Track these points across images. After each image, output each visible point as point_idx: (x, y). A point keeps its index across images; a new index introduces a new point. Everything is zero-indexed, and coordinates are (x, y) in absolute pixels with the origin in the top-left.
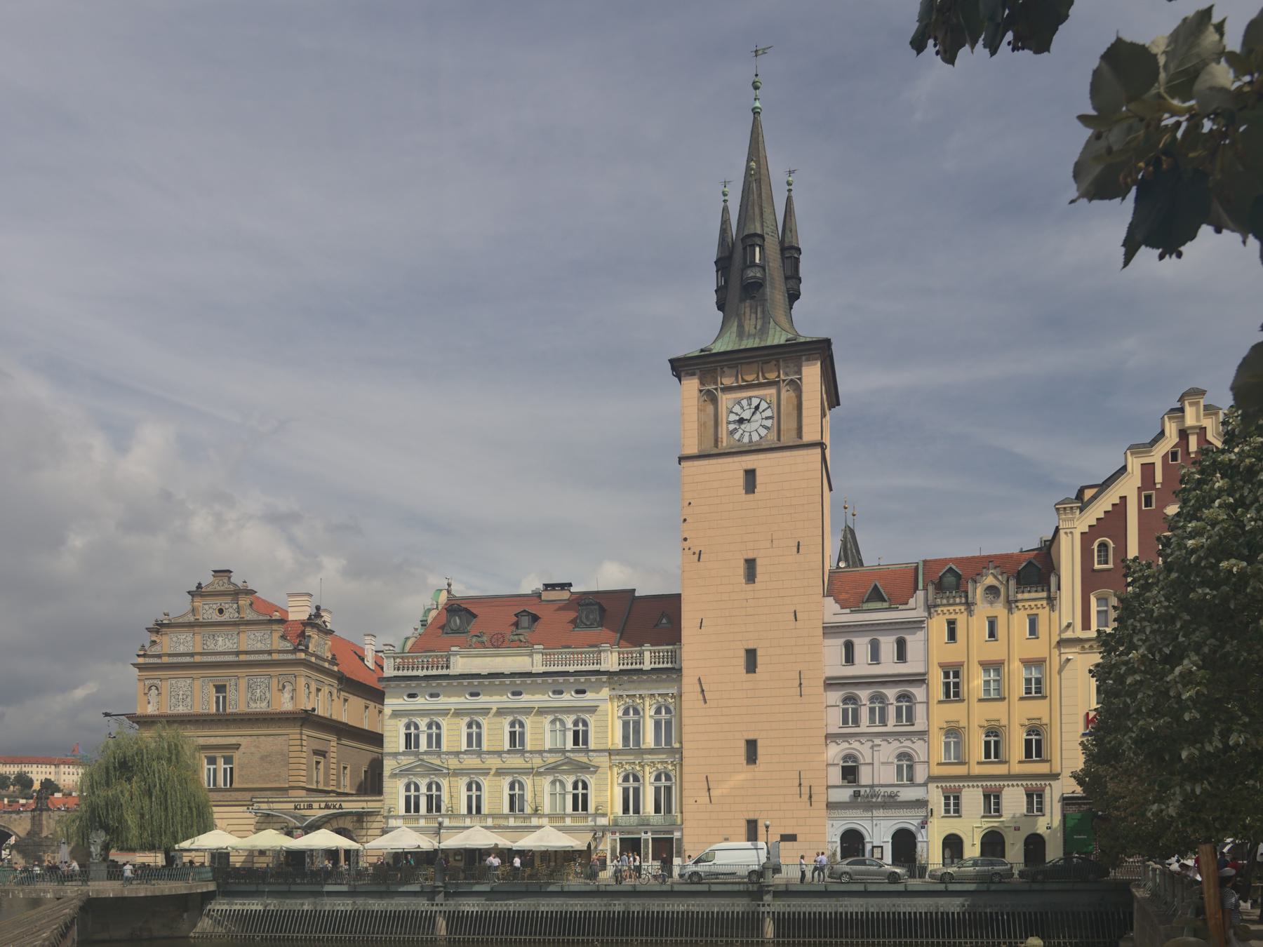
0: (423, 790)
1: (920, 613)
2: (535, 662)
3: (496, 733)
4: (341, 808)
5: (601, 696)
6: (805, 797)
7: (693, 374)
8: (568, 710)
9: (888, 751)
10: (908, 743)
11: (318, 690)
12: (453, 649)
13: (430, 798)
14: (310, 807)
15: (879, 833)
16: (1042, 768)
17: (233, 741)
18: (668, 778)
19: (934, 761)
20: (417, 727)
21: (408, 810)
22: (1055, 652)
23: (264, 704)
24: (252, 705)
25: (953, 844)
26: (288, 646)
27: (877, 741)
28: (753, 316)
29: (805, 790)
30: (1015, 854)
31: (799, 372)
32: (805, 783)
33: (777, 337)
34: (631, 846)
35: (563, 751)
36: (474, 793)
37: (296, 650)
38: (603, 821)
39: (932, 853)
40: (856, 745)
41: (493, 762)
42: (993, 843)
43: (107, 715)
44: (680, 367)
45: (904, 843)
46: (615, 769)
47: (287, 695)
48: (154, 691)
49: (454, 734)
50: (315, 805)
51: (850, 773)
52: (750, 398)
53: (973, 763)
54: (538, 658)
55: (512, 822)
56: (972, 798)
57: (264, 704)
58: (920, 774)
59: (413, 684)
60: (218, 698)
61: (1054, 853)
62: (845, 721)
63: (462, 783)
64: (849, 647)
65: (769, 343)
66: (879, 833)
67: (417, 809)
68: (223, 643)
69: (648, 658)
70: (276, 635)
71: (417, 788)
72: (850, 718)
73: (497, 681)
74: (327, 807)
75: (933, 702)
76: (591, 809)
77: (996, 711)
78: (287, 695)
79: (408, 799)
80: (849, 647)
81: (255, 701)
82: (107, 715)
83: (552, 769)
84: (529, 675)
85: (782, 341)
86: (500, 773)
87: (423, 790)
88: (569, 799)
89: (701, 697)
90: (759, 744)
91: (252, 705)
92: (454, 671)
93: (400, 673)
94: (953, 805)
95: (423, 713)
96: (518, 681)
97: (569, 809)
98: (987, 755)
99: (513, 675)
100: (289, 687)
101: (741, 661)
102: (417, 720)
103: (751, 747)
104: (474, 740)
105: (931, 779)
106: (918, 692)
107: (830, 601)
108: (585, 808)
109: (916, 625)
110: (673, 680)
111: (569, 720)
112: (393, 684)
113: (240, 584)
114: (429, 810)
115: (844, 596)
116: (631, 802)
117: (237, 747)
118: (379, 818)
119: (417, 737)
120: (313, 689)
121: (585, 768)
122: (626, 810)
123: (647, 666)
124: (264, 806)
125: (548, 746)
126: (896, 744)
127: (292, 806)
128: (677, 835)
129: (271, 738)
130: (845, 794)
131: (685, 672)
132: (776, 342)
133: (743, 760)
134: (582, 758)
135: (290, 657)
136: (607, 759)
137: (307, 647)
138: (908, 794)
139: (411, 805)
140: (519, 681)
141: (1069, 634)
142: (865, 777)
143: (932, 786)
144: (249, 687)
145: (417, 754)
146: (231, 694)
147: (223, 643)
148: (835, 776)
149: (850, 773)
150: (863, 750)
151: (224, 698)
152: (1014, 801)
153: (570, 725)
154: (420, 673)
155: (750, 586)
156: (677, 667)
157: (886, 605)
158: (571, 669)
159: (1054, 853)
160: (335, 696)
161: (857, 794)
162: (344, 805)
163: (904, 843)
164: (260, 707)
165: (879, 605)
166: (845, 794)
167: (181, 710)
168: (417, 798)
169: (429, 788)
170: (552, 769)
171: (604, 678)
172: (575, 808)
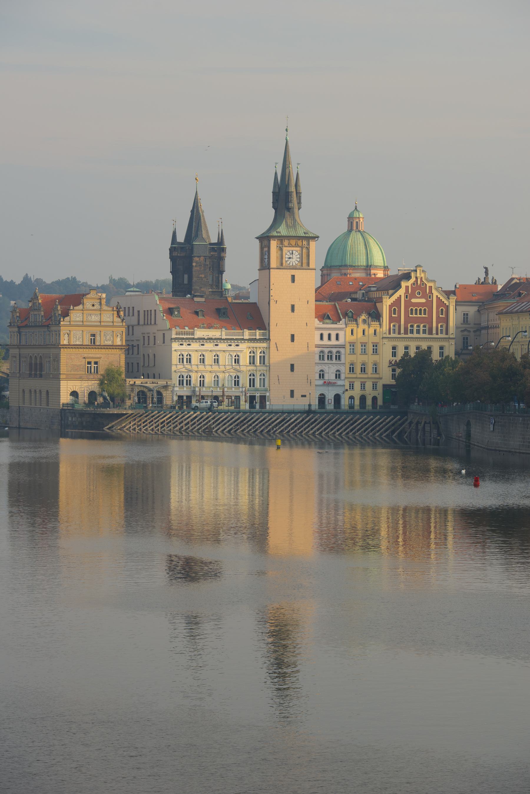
1: (344, 326)
3: (209, 359)
4: (157, 383)
5: (243, 346)
6: (309, 383)
10: (339, 367)
12: (196, 329)
13: (187, 380)
14: (146, 383)
15: (330, 396)
16: (377, 376)
17: (98, 356)
18: (264, 375)
19: (346, 373)
20: (183, 355)
21: (179, 385)
22: (381, 340)
27: (330, 366)
29: (309, 381)
30: (369, 402)
36: (202, 379)
39: (345, 402)
40: (324, 367)
41: (208, 368)
42: (363, 398)
45: (337, 398)
47: (119, 339)
49: (195, 359)
50: (149, 382)
51: (322, 376)
53: (358, 373)
54: (223, 333)
56: (357, 385)
58: (343, 376)
60: (91, 339)
61: (380, 402)
62: (320, 359)
64: (322, 335)
66: (330, 396)
67: (183, 384)
71: (183, 377)
72: (321, 357)
74: (153, 383)
75: (347, 355)
76: (240, 385)
77: (364, 358)
79: (180, 380)
80: (322, 335)
84: (221, 339)
88: (233, 381)
91: (106, 342)
92: (196, 337)
93: (177, 336)
94: (352, 386)
95: (185, 350)
97: (233, 386)
98: (362, 372)
99: (215, 339)
102: (183, 353)
104: (203, 361)
106: (342, 350)
107: (317, 319)
108: (238, 385)
114: (187, 385)
116: (252, 382)
117: (100, 358)
119: (183, 359)
122: (250, 386)
123: (258, 337)
126: (335, 367)
128: (268, 394)
129: (113, 355)
130: (321, 382)
134: (238, 367)
139: (181, 383)
140: (217, 340)
141: (385, 336)
142: (326, 377)
143: (346, 380)
144: (104, 335)
146: (98, 338)
149: (322, 376)
150: (325, 368)
151: (94, 339)
152: (369, 385)
153: (234, 357)
154: (185, 337)
156: (267, 338)
158: (234, 337)
159: (380, 402)
162: (159, 382)
163: (337, 398)
164: (110, 343)
166: (321, 382)
167: (78, 343)
168: (183, 380)
169: (187, 377)
171: (246, 341)
172: (235, 385)
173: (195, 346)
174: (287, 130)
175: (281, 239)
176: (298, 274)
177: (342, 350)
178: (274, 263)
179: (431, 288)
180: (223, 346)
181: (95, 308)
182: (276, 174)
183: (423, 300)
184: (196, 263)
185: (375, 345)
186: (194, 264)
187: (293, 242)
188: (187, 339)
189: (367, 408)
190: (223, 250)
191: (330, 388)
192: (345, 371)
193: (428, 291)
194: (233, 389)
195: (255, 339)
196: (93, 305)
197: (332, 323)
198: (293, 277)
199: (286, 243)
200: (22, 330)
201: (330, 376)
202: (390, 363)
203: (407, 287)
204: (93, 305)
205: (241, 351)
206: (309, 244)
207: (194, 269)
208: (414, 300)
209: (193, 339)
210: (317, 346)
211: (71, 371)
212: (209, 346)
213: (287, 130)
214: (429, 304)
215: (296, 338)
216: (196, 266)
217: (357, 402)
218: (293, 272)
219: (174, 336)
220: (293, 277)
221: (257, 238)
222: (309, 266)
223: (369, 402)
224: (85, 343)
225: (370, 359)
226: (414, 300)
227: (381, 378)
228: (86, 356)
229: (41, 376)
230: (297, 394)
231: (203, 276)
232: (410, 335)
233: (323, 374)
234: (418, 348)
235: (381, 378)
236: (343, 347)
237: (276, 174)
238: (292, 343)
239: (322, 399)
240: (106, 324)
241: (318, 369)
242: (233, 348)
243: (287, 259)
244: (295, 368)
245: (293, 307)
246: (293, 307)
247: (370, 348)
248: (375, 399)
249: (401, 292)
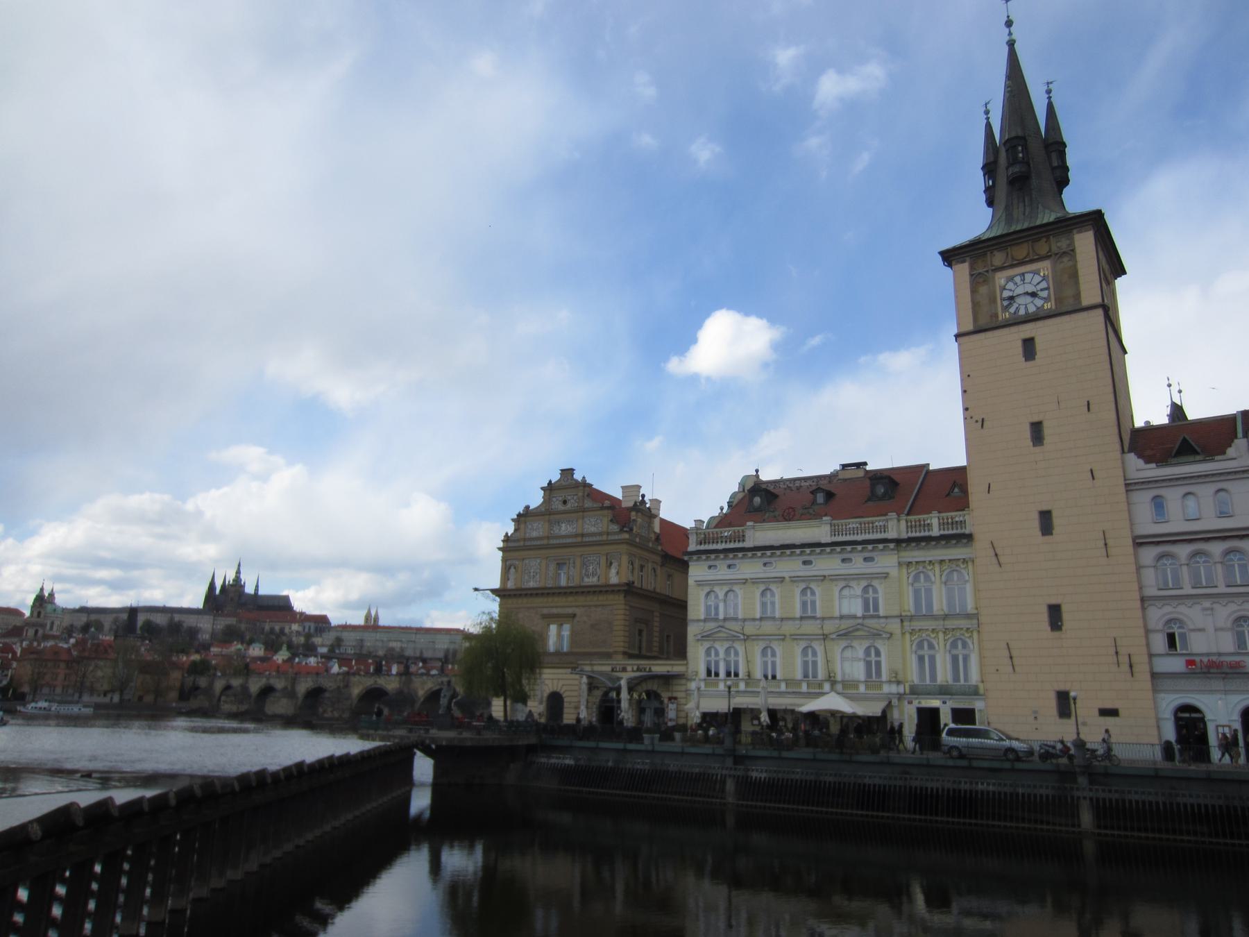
0: (722, 655)
2: (820, 531)
6: (1125, 667)
7: (964, 262)
8: (858, 577)
11: (642, 567)
14: (624, 670)
17: (570, 611)
23: (595, 579)
24: (586, 580)
26: (615, 528)
27: (1207, 604)
28: (1021, 205)
29: (1124, 660)
31: (1072, 240)
32: (1122, 651)
33: (1048, 217)
34: (929, 718)
35: (855, 617)
37: (621, 531)
38: (894, 689)
40: (1182, 609)
43: (476, 589)
44: (950, 257)
46: (908, 636)
48: (512, 570)
50: (629, 668)
52: (1023, 274)
54: (827, 528)
55: (804, 688)
57: (595, 579)
59: (713, 556)
63: (757, 648)
64: (1158, 503)
65: (1038, 222)
68: (565, 529)
69: (934, 524)
70: (606, 520)
71: (717, 654)
73: (788, 552)
74: (639, 670)
78: (613, 571)
81: (588, 576)
82: (476, 589)
84: (819, 545)
85: (1052, 219)
86: (796, 637)
87: (722, 655)
89: (994, 560)
90: (1064, 608)
91: (586, 580)
92: (747, 544)
93: (702, 547)
96: (808, 551)
100: (615, 565)
101: (1035, 523)
103: (1055, 613)
107: (1131, 457)
110: (966, 545)
111: (858, 590)
112: (695, 557)
113: (580, 479)
115: (1149, 452)
117: (574, 616)
118: (683, 681)
120: (637, 565)
121: (876, 635)
123: (935, 532)
124: (588, 668)
125: (837, 614)
126: (1233, 607)
127: (608, 669)
128: (978, 705)
130: (1175, 664)
131: (976, 537)
132: (1045, 221)
133: (1045, 625)
135: (616, 537)
136: (899, 625)
137: (631, 530)
145: (716, 620)
147: (565, 529)
148: (1160, 643)
150: (1193, 615)
154: (720, 546)
155: (1038, 449)
156: (967, 532)
157: (1198, 458)
158: (859, 538)
160: (658, 571)
161: (1190, 663)
164: (592, 581)
165: (1191, 458)
167: (532, 584)
169: (727, 651)
170: (845, 635)
171: (892, 546)
173: (750, 568)
176: (1042, 332)
180: (828, 564)
181: (569, 506)
182: (989, 127)
187: (1021, 251)
188: (726, 551)
191: (1218, 684)
194: (862, 688)
195: (928, 539)
196: (565, 502)
197: (1204, 461)
198: (1029, 347)
199: (998, 258)
204: (565, 502)
205: (886, 576)
206: (1072, 243)
210: (1139, 542)
212: (788, 567)
213: (1009, 24)
215: (1057, 521)
218: (1027, 331)
219: (692, 547)
220: (1029, 347)
222: (1080, 302)
224: (542, 585)
228: (545, 611)
230: (1086, 708)
233: (1183, 636)
237: (989, 127)
238: (1047, 538)
239: (1190, 724)
240: (591, 539)
241: (1157, 615)
242: (858, 565)
243: (1006, 303)
244: (1066, 616)
245: (1037, 432)
246: (1037, 432)
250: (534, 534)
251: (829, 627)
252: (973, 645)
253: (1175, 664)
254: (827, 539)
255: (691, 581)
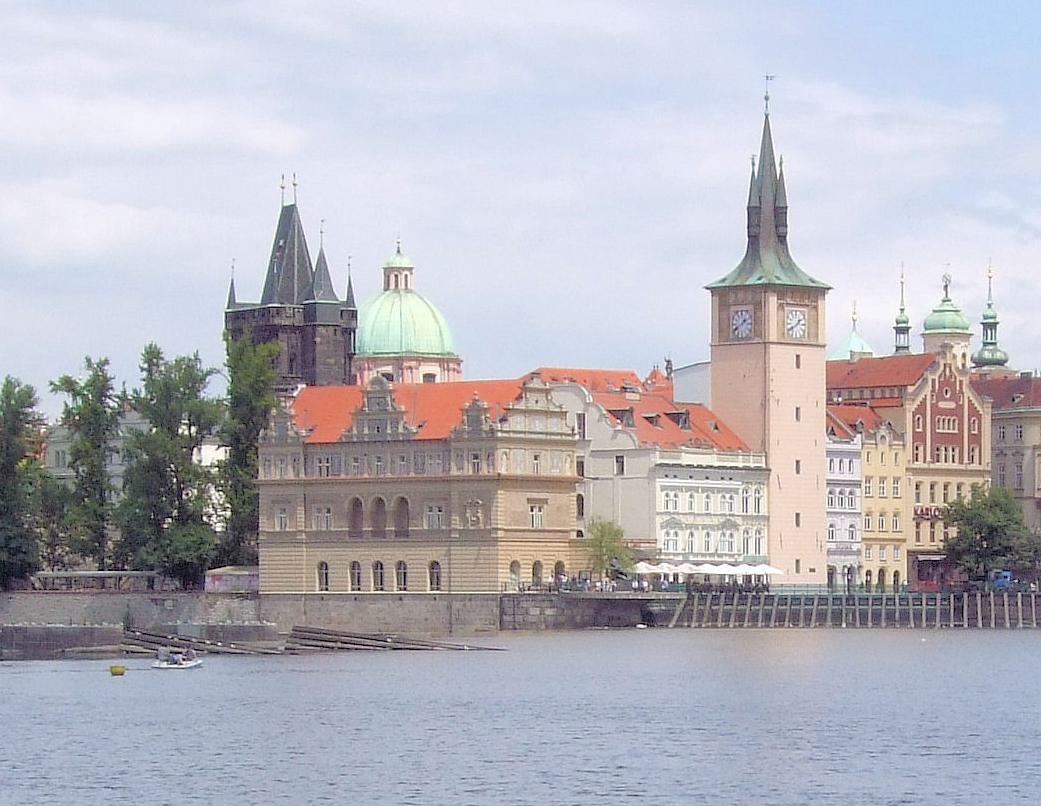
9: (848, 521)
25: (869, 573)
27: (843, 517)
30: (889, 580)
35: (725, 515)
42: (882, 572)
51: (832, 535)
83: (723, 526)
92: (684, 463)
105: (863, 539)
109: (857, 454)
138: (855, 547)
156: (764, 466)
157: (836, 439)
159: (903, 579)
170: (723, 526)
174: (767, 98)
175: (782, 291)
176: (803, 352)
177: (857, 491)
178: (773, 336)
179: (961, 382)
183: (952, 405)
184: (322, 336)
185: (896, 480)
186: (318, 340)
189: (887, 589)
190: (354, 315)
192: (859, 523)
193: (958, 388)
195: (749, 469)
196: (537, 402)
200: (311, 449)
201: (842, 535)
202: (916, 513)
203: (933, 380)
204: (537, 402)
207: (318, 348)
208: (942, 405)
209: (680, 466)
211: (510, 525)
213: (767, 98)
214: (957, 412)
216: (321, 343)
217: (875, 581)
221: (713, 290)
223: (889, 580)
225: (890, 506)
226: (942, 405)
227: (904, 540)
229: (406, 534)
231: (332, 361)
232: (937, 465)
234: (974, 487)
235: (904, 540)
236: (857, 484)
247: (889, 485)
248: (896, 574)
249: (928, 390)
250: (519, 428)
251: (715, 521)
252: (765, 533)
253: (833, 546)
254: (716, 464)
255: (658, 486)
